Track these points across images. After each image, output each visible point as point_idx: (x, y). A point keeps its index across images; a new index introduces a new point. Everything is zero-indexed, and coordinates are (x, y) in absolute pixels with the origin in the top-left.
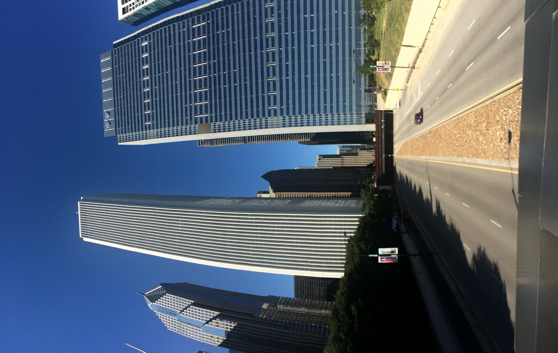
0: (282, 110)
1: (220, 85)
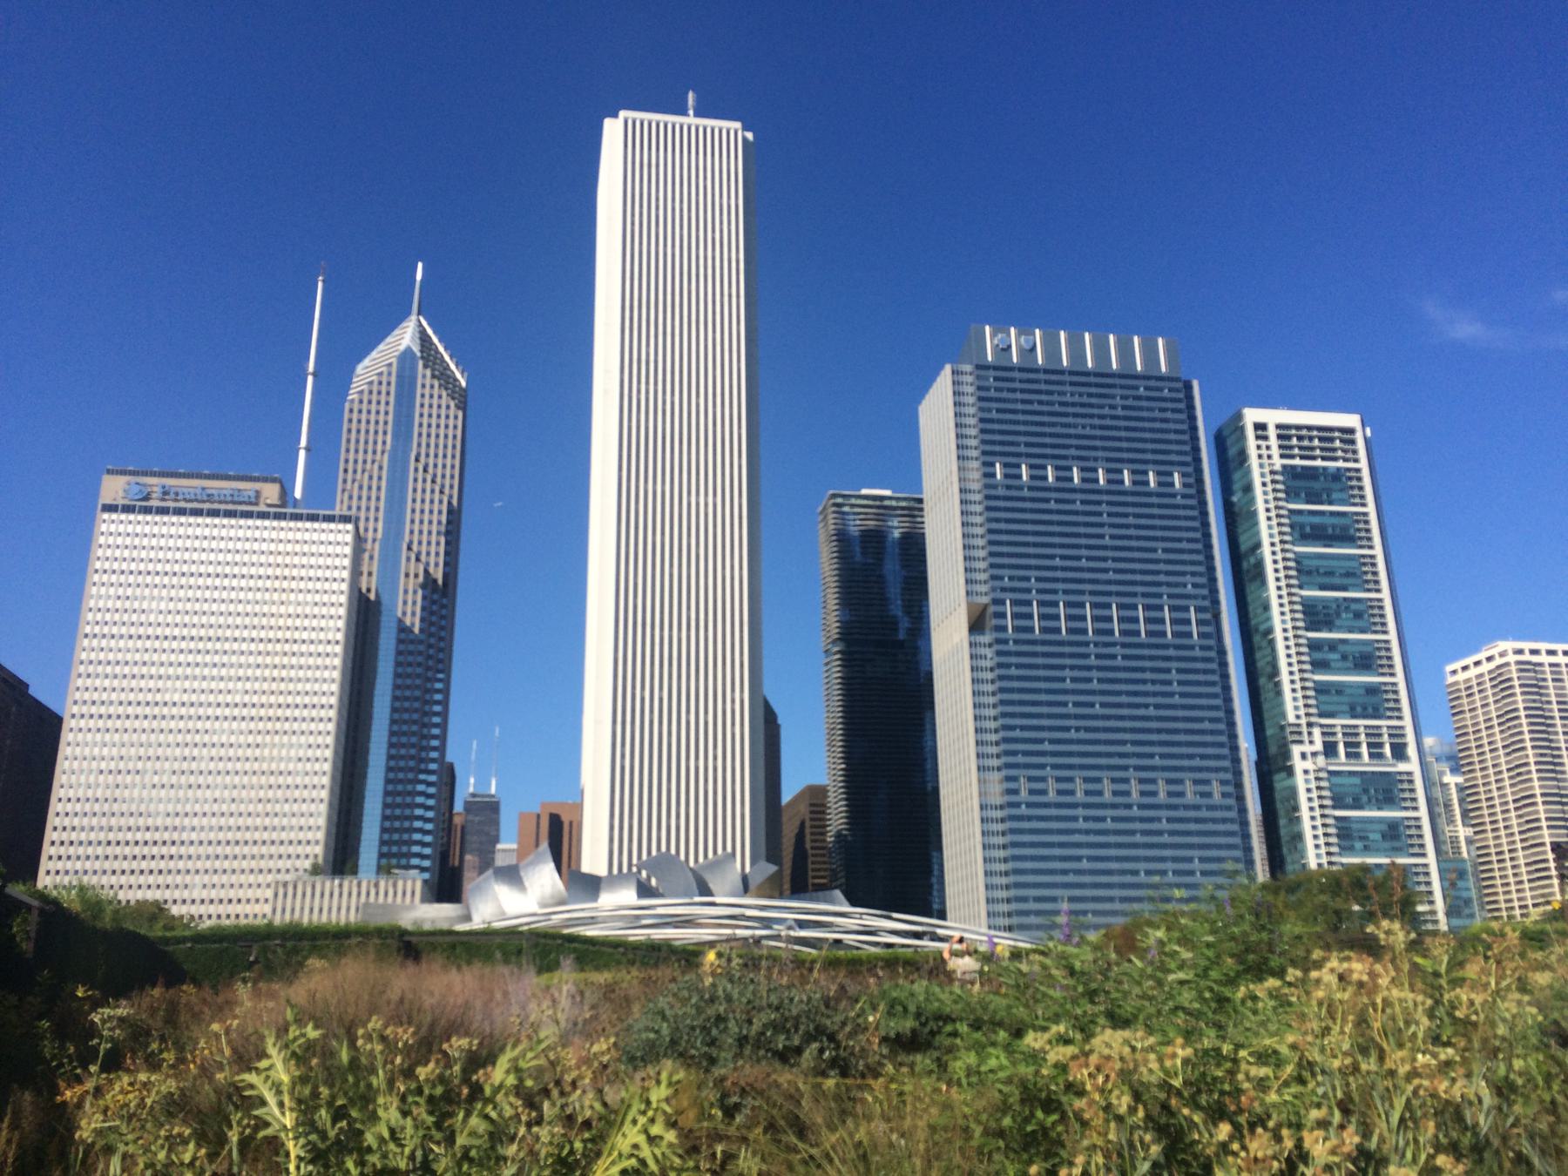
0: (1018, 805)
1: (1072, 668)
